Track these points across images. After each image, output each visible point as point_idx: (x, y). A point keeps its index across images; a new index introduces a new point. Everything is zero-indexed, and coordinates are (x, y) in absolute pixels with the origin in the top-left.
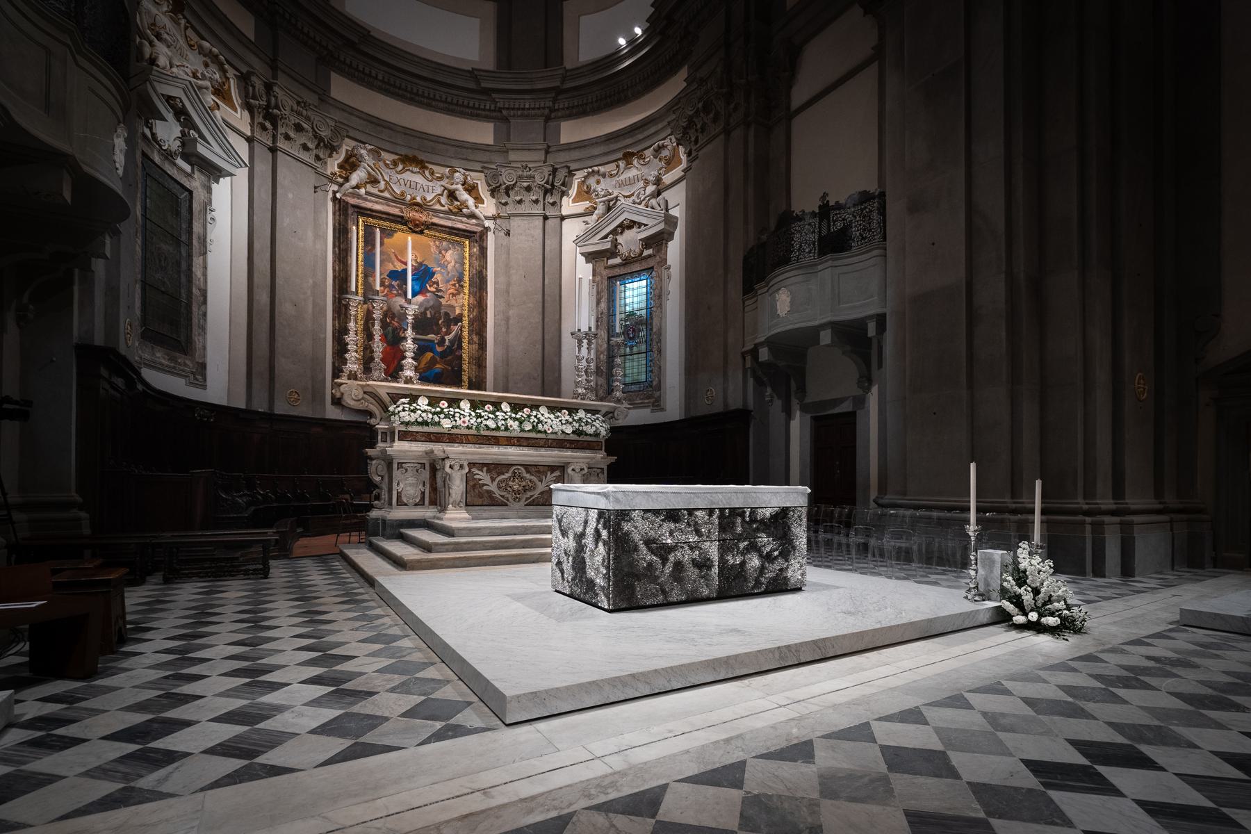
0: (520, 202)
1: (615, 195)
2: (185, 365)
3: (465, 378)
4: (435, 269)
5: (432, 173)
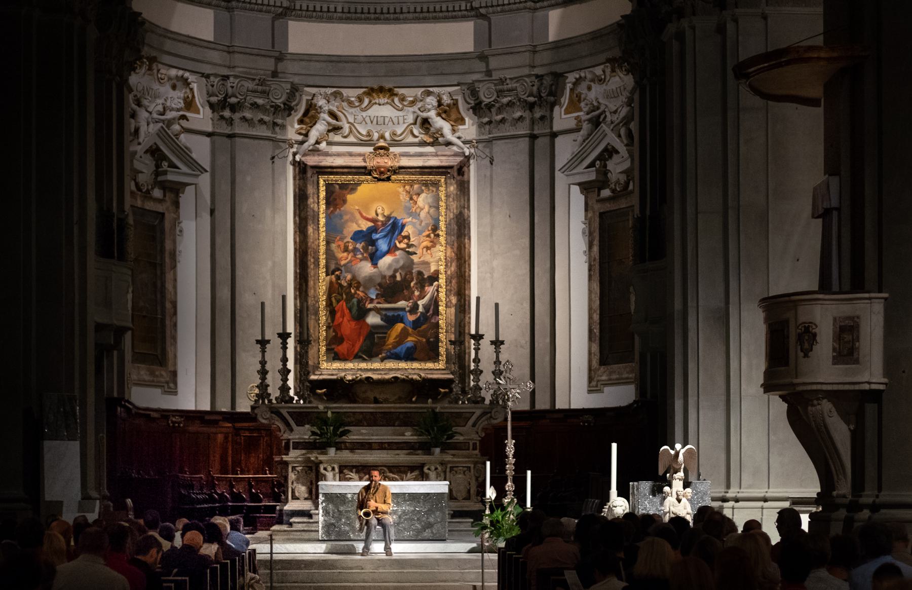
0: (503, 121)
1: (602, 108)
2: (162, 375)
3: (442, 350)
4: (404, 221)
5: (402, 99)
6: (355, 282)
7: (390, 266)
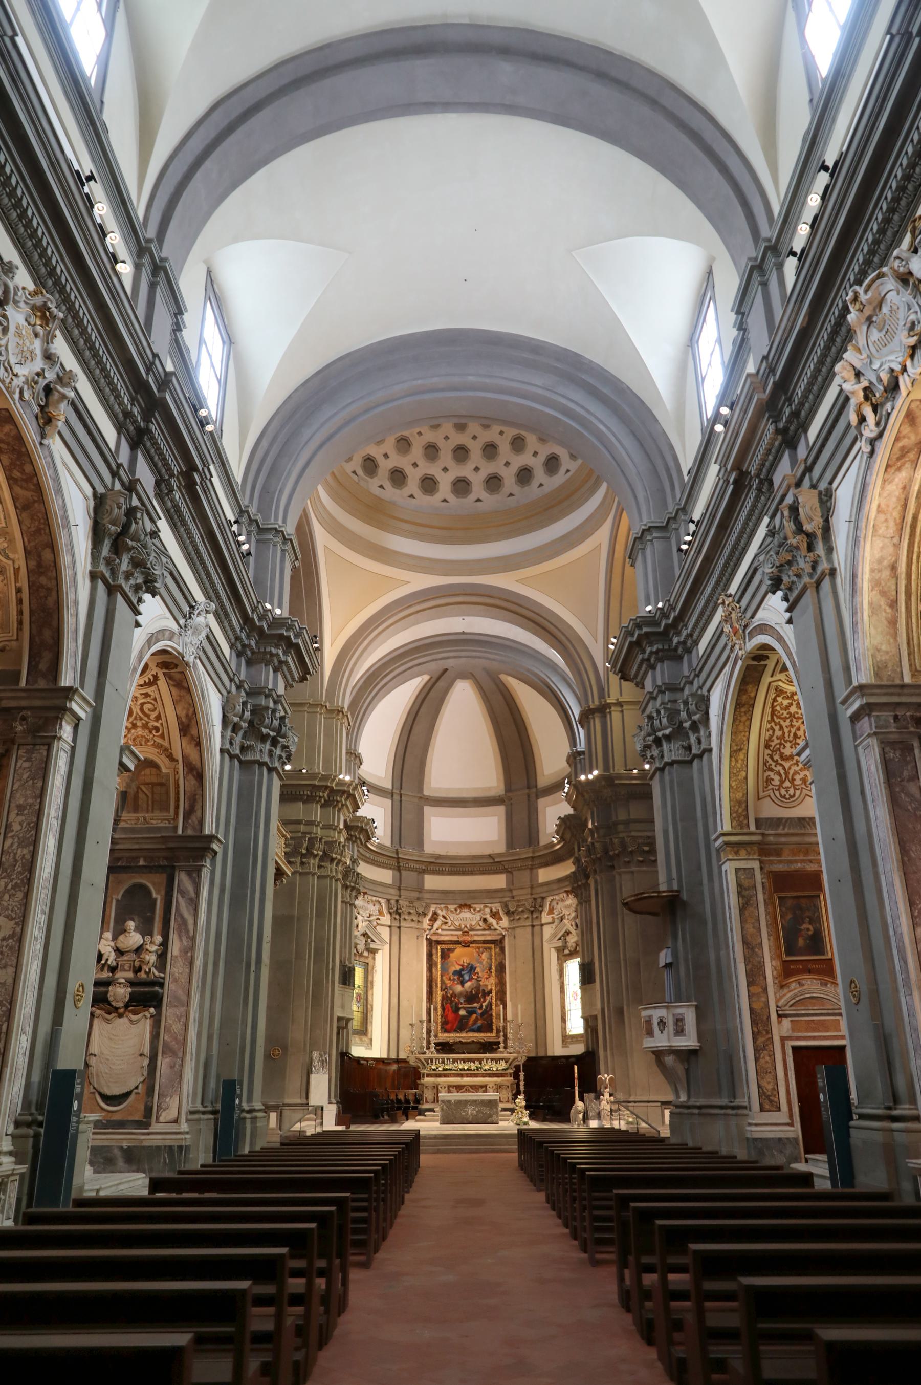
0: (519, 919)
3: (494, 1028)
5: (475, 909)
6: (454, 995)
7: (470, 987)
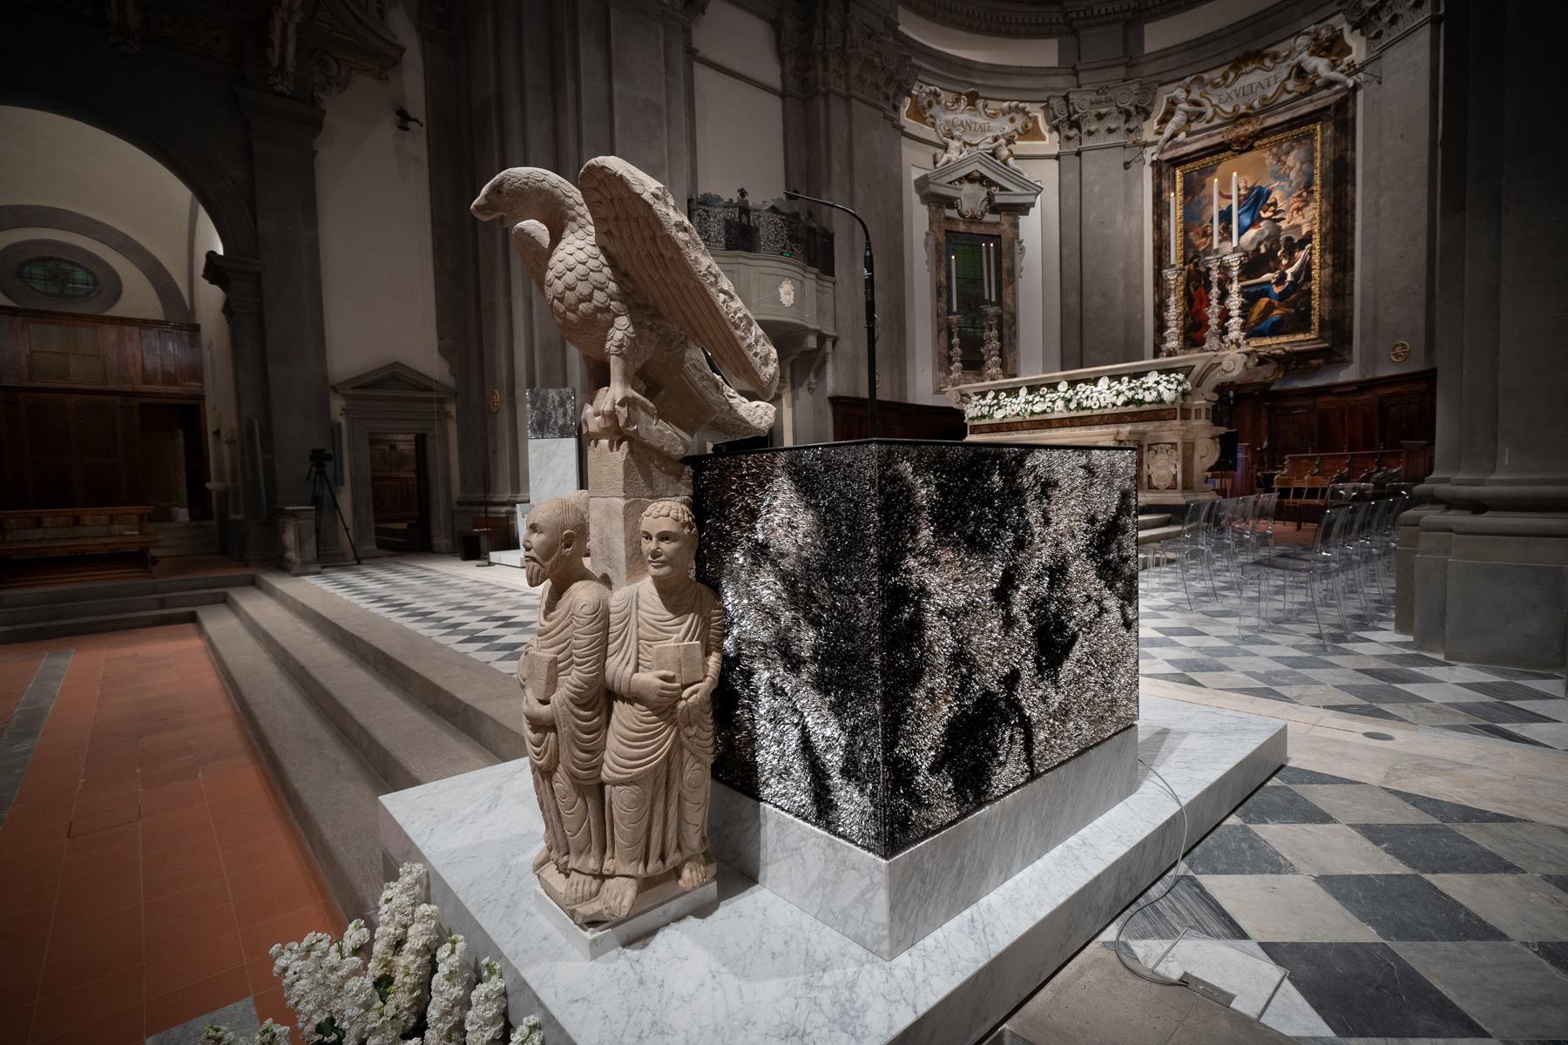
3: (1315, 319)
5: (1275, 57)
7: (1253, 239)
